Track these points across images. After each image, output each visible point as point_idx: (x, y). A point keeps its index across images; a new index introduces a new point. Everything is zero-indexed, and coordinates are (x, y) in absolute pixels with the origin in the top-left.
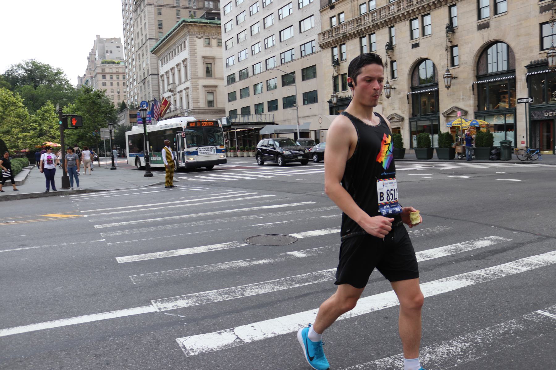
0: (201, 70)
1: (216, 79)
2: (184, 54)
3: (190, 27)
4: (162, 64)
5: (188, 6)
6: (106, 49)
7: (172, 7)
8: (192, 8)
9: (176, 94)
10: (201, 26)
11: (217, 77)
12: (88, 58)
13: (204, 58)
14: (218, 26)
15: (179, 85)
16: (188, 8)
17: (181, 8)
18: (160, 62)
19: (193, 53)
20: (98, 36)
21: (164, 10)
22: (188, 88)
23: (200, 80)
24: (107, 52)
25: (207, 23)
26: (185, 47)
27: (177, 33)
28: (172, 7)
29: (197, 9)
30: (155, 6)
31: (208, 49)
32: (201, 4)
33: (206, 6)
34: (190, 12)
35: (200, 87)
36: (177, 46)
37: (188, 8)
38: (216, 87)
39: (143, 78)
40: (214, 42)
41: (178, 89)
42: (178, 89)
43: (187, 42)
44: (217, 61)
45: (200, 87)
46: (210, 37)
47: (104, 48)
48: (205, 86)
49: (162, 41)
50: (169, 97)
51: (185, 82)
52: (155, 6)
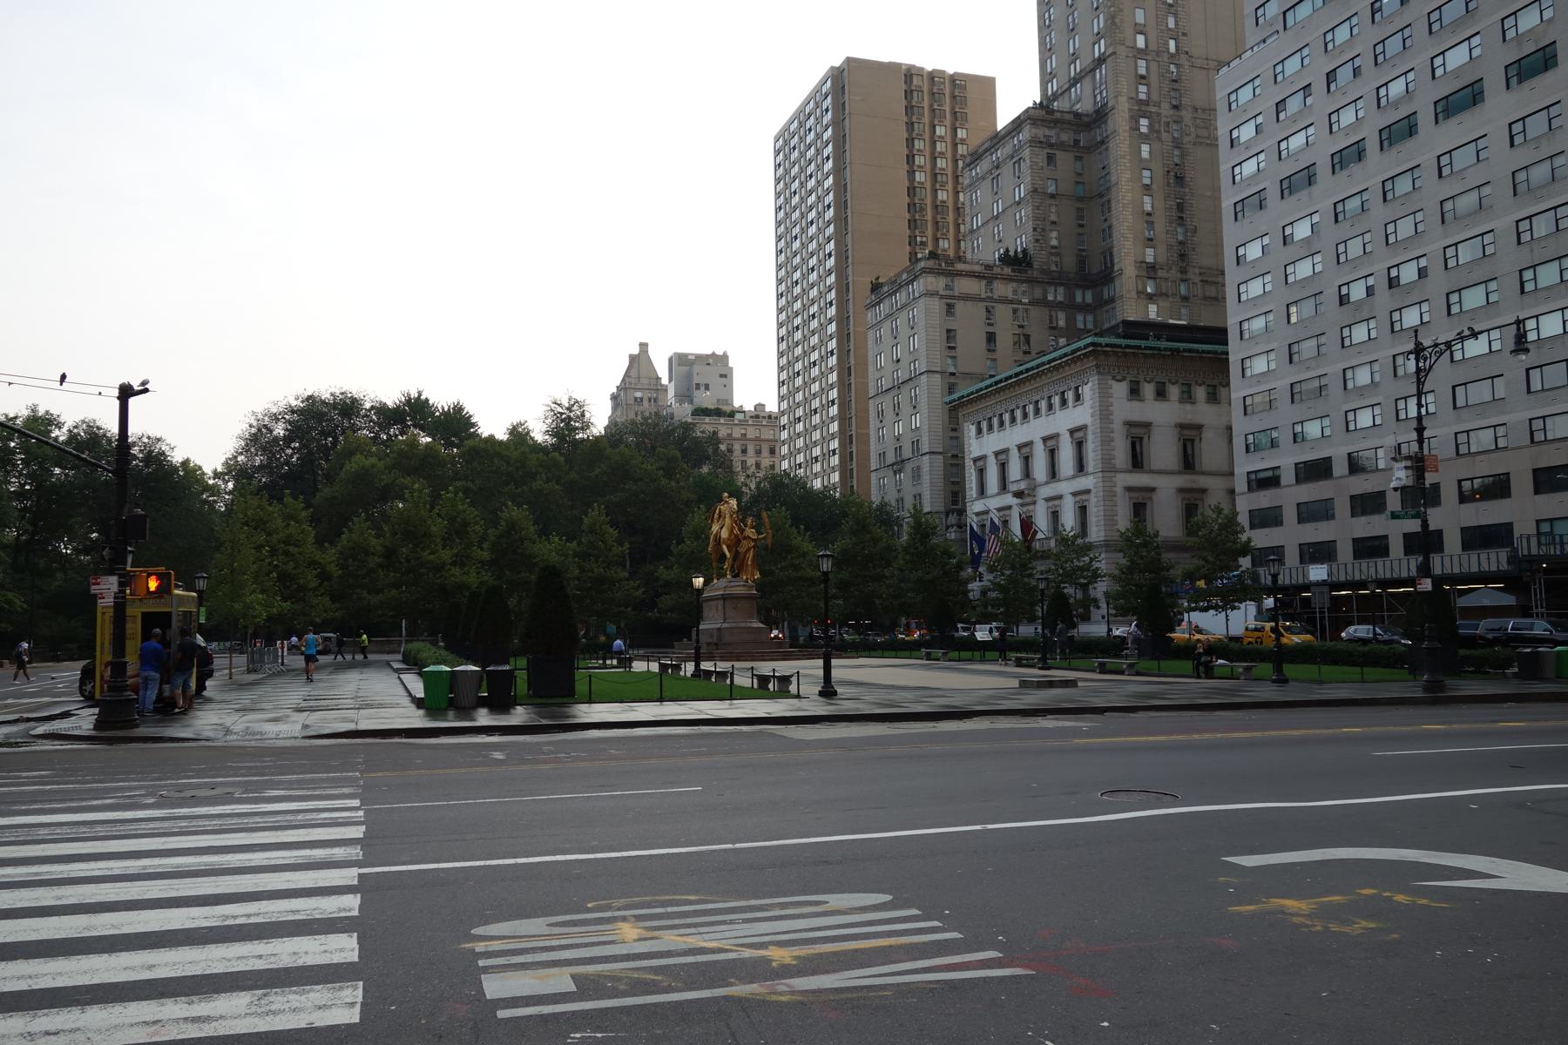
0: (1121, 454)
1: (1151, 472)
2: (1081, 414)
3: (1102, 357)
4: (979, 431)
5: (1010, 296)
6: (696, 380)
7: (979, 299)
8: (1020, 303)
9: (1034, 503)
10: (1125, 354)
11: (1155, 465)
12: (614, 398)
13: (1130, 424)
14: (1221, 362)
15: (1047, 483)
16: (1012, 302)
17: (996, 301)
18: (973, 428)
19: (1104, 413)
20: (644, 346)
21: (960, 307)
22: (1088, 492)
23: (1119, 476)
24: (698, 386)
25: (1139, 347)
26: (1078, 397)
27: (1056, 368)
28: (979, 299)
29: (1030, 303)
30: (942, 297)
31: (1136, 404)
32: (1038, 293)
33: (1050, 298)
34: (1015, 311)
35: (1119, 490)
36: (1046, 394)
37: (1012, 302)
38: (1153, 490)
39: (891, 458)
40: (1148, 390)
41: (1045, 492)
42: (1045, 492)
43: (1087, 391)
44: (1155, 430)
45: (1119, 490)
46: (1141, 378)
47: (689, 376)
48: (1129, 489)
49: (996, 383)
50: (1010, 507)
51: (1074, 477)
52: (942, 297)
